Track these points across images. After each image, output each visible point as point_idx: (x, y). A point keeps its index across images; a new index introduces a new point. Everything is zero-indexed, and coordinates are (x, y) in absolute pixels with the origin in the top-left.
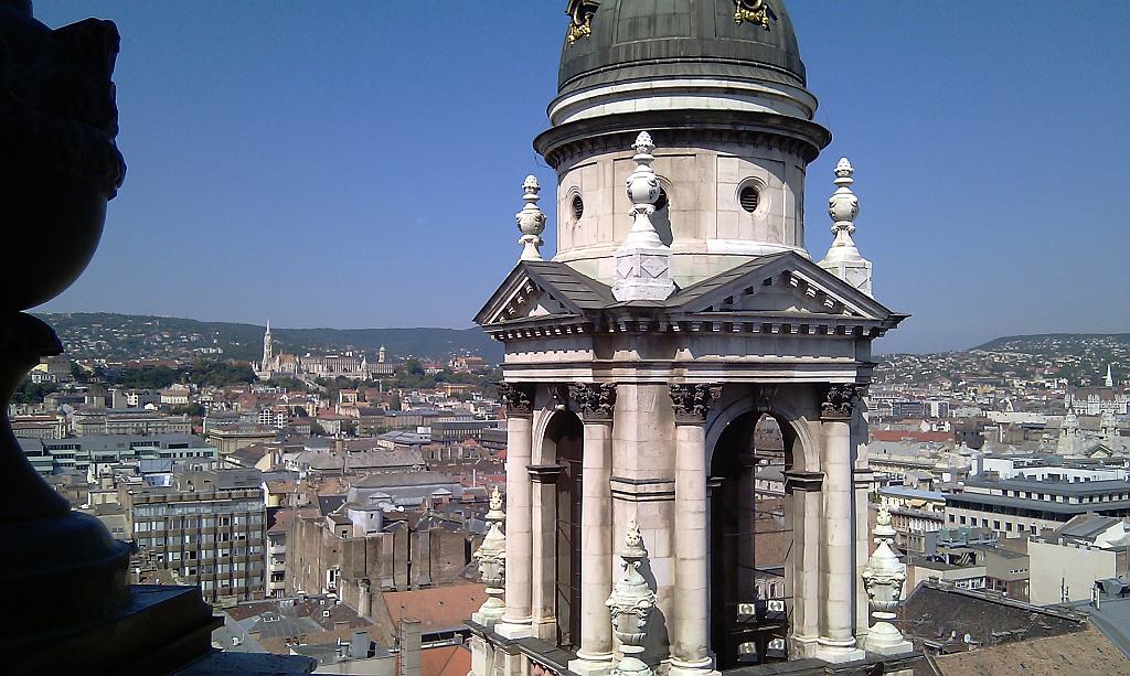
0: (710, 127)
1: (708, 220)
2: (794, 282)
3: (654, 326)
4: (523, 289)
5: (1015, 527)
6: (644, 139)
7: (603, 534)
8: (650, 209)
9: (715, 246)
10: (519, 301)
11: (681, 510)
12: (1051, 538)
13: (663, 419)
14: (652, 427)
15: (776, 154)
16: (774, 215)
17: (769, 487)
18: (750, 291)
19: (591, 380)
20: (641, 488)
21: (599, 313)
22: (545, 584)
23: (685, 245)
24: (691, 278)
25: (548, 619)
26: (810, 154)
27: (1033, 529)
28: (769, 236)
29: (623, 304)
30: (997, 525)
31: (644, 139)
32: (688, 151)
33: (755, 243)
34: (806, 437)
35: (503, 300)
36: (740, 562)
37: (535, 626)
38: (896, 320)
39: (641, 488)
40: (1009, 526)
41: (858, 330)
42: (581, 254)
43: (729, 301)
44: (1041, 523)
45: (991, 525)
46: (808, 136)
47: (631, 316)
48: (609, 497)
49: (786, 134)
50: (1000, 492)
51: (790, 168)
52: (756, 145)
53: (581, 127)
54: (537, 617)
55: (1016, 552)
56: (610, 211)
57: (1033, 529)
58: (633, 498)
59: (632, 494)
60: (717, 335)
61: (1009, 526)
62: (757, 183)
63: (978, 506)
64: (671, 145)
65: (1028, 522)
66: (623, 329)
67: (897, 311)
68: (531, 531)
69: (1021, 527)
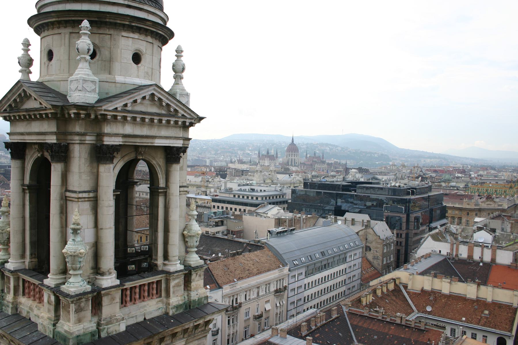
0: (119, 22)
1: (117, 66)
2: (156, 99)
3: (88, 115)
4: (20, 94)
5: (238, 210)
6: (85, 23)
7: (61, 218)
8: (88, 58)
9: (119, 79)
10: (18, 100)
11: (100, 205)
12: (251, 213)
13: (91, 162)
14: (87, 165)
15: (149, 39)
16: (147, 67)
17: (140, 195)
18: (135, 101)
19: (55, 142)
20: (81, 195)
21: (60, 107)
22: (31, 243)
23: (105, 77)
24: (107, 93)
25: (33, 260)
26: (164, 41)
27: (245, 211)
28: (145, 77)
29: (73, 104)
30: (231, 209)
31: (85, 23)
32: (107, 31)
33: (139, 79)
34: (160, 171)
35: (9, 100)
36: (128, 229)
37: (27, 263)
38: (200, 119)
39: (81, 195)
40: (236, 210)
41: (184, 123)
42: (52, 78)
43: (126, 105)
44: (248, 208)
45: (229, 209)
46: (164, 33)
47: (76, 110)
48: (65, 200)
49: (154, 30)
50: (232, 196)
51: (155, 47)
52: (140, 34)
53: (53, 14)
54: (27, 260)
55: (239, 218)
56: (67, 58)
57: (245, 211)
58: (77, 200)
59: (76, 198)
60: (119, 122)
61: (236, 210)
62: (139, 51)
63: (224, 202)
64: (99, 28)
65: (243, 208)
66: (72, 116)
67: (201, 115)
68: (24, 217)
69: (240, 210)
